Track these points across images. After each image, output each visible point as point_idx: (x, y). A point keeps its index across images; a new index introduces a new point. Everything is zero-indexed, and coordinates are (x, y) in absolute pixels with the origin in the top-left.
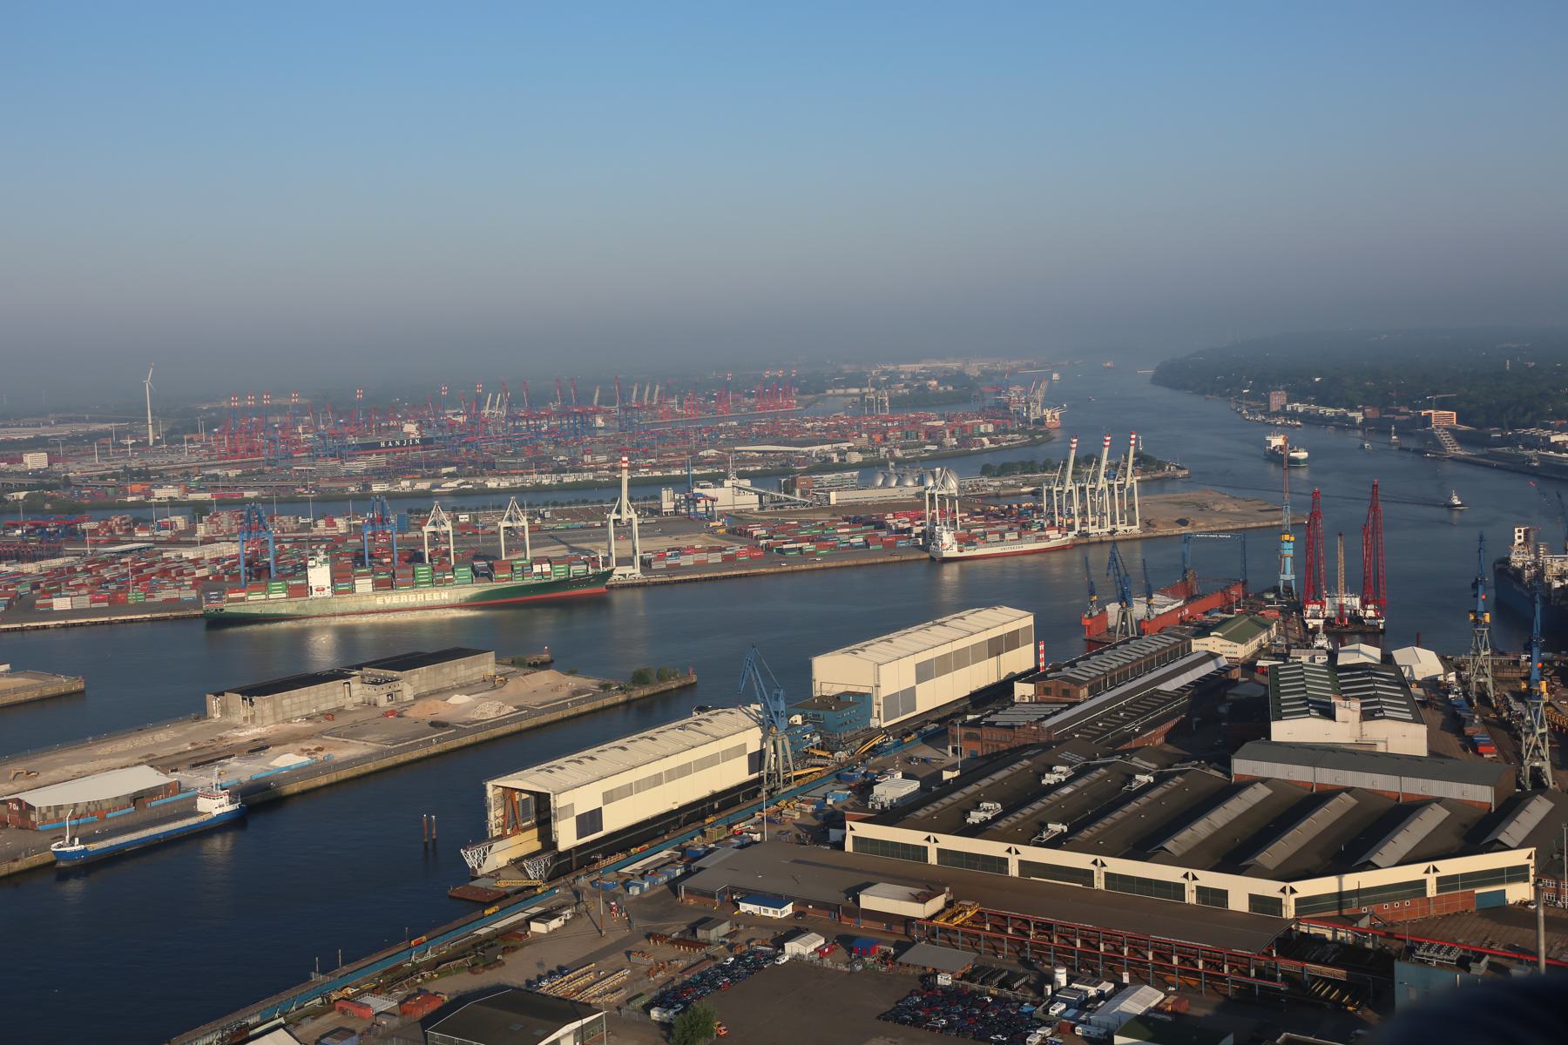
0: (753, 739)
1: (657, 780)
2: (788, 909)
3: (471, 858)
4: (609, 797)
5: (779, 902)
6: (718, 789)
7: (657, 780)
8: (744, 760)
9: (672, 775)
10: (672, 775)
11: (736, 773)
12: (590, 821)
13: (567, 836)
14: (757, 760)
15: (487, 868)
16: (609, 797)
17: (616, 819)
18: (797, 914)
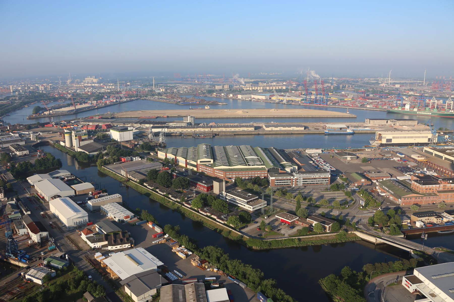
0: (430, 136)
1: (405, 137)
2: (403, 156)
3: (371, 142)
4: (394, 138)
5: (402, 154)
6: (420, 142)
7: (405, 137)
8: (427, 139)
9: (408, 137)
10: (408, 137)
11: (426, 141)
12: (389, 140)
13: (384, 141)
14: (429, 139)
15: (373, 144)
16: (394, 138)
17: (394, 141)
18: (405, 157)
